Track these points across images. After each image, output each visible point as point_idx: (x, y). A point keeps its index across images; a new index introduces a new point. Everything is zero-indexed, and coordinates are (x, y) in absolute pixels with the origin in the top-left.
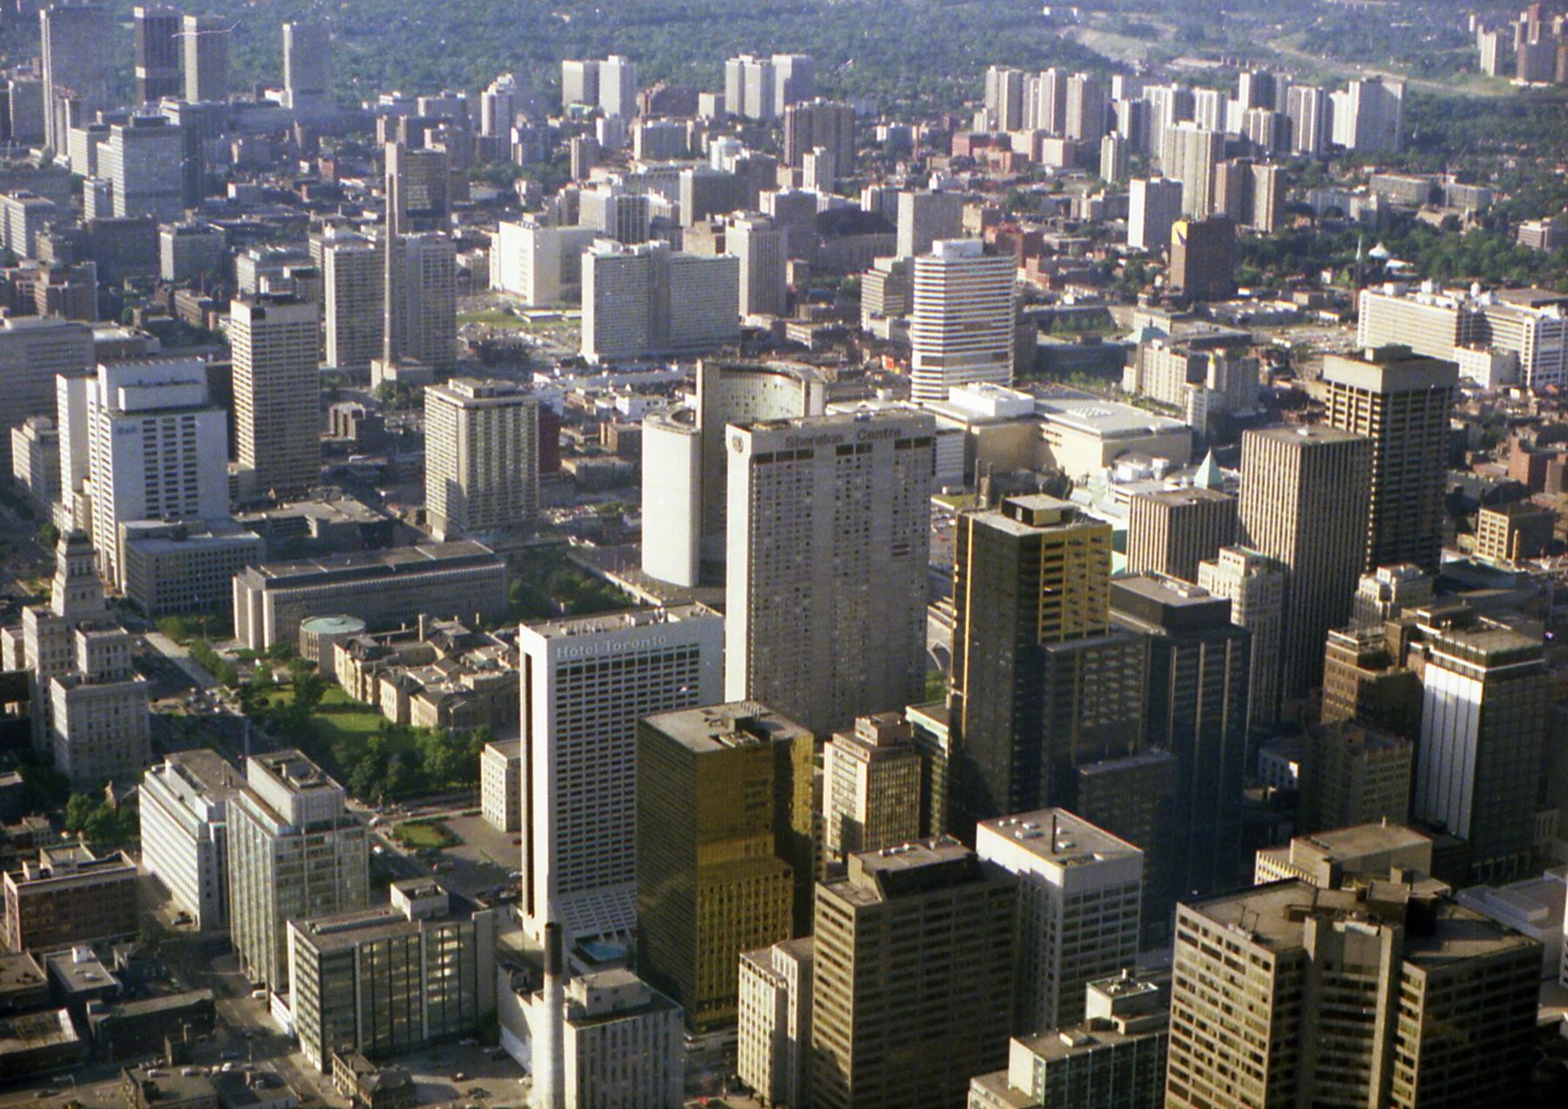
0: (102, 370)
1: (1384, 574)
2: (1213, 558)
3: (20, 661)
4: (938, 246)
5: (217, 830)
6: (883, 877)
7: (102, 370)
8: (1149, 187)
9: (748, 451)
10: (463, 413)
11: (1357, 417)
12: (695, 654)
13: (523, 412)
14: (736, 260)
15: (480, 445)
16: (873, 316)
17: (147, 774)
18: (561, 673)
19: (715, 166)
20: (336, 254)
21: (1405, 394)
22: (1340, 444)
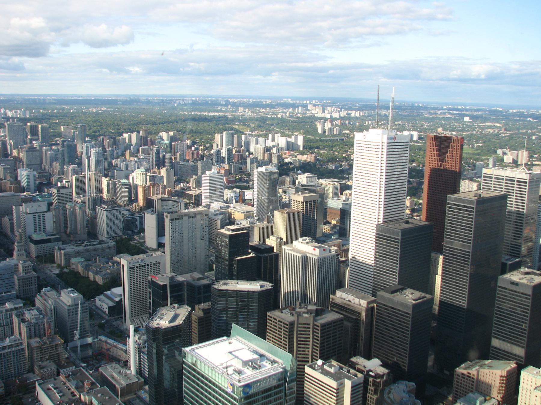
0: (23, 204)
2: (269, 238)
4: (207, 172)
6: (203, 310)
7: (23, 204)
8: (251, 159)
12: (159, 263)
14: (163, 176)
18: (130, 268)
22: (442, 278)
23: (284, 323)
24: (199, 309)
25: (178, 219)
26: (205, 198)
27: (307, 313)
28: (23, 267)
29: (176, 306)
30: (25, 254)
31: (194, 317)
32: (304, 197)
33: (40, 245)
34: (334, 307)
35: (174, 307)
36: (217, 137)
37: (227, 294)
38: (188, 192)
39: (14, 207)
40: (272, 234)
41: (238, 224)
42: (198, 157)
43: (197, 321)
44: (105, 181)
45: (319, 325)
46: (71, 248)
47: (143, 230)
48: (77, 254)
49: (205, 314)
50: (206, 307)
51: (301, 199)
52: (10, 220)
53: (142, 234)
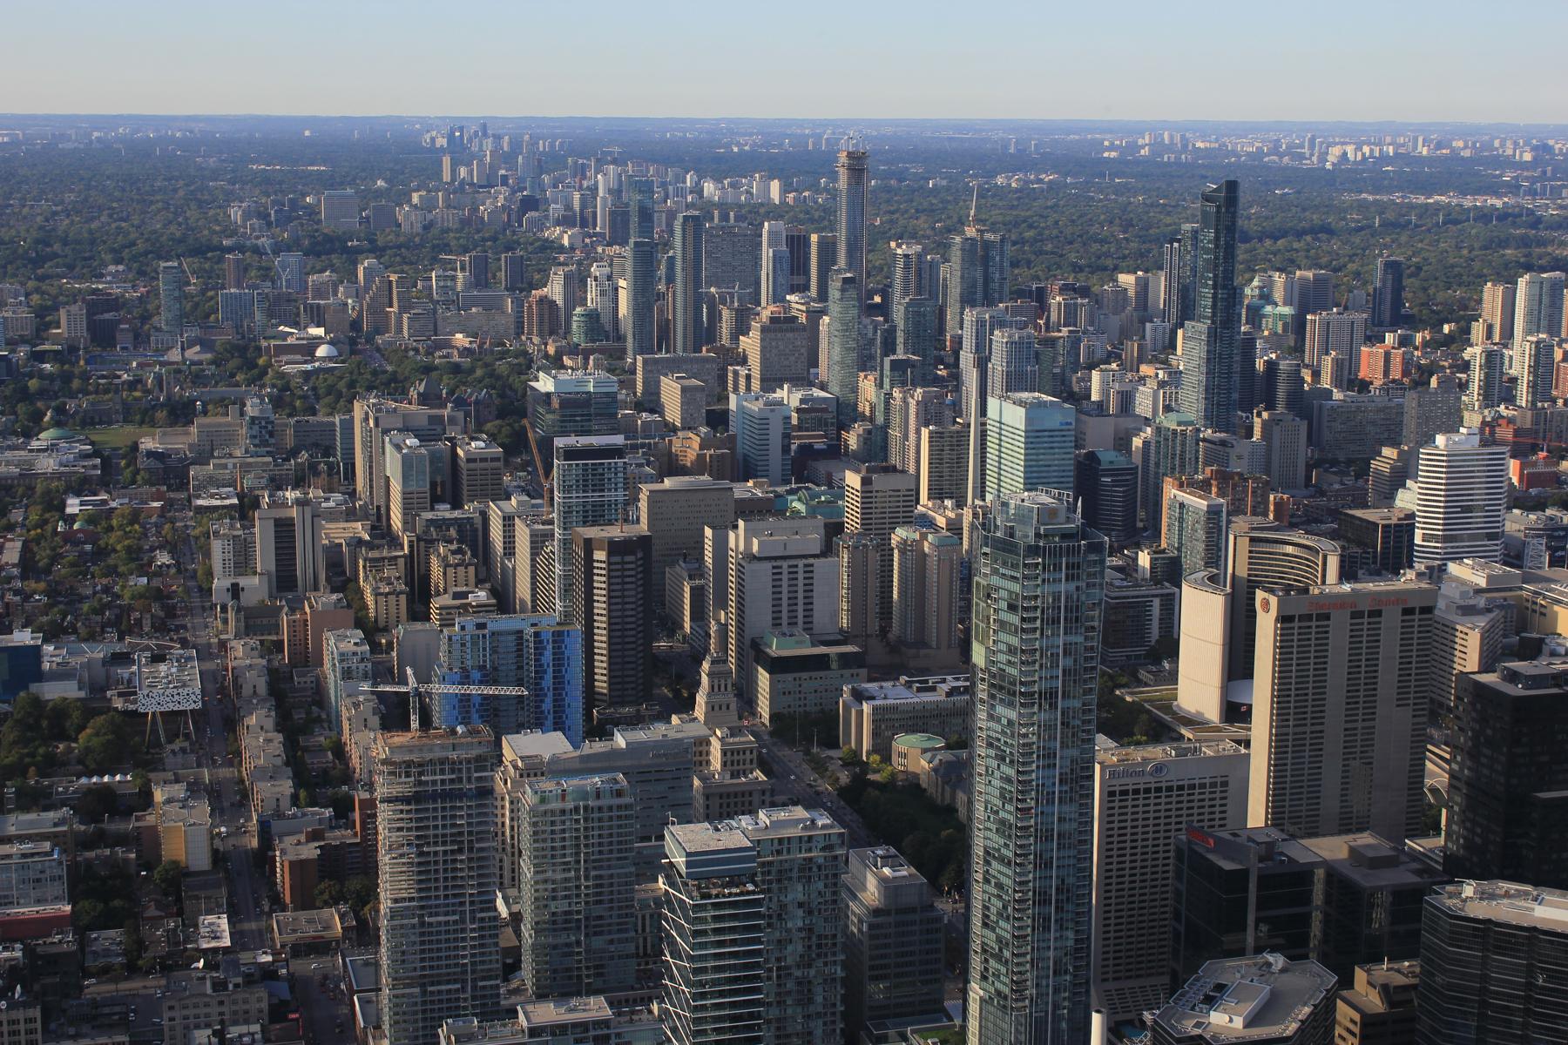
4: (1440, 440)
7: (741, 523)
12: (1225, 784)
18: (1112, 794)
20: (931, 432)
26: (1425, 538)
28: (724, 753)
29: (1277, 961)
30: (733, 706)
31: (1344, 1012)
33: (789, 677)
35: (1269, 965)
36: (1492, 295)
37: (1490, 934)
38: (1358, 513)
39: (708, 532)
41: (1553, 654)
42: (1405, 373)
43: (1356, 1030)
46: (897, 693)
47: (1169, 646)
48: (916, 721)
50: (1401, 980)
53: (1167, 665)
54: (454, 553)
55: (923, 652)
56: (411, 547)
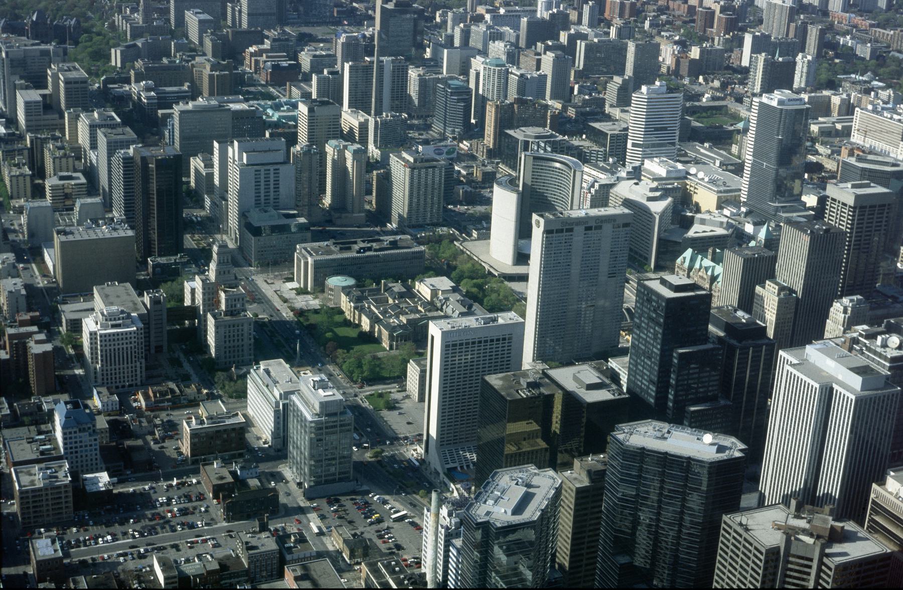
0: (236, 143)
1: (846, 301)
3: (193, 300)
4: (644, 89)
5: (284, 405)
7: (236, 143)
8: (755, 38)
9: (542, 228)
10: (408, 170)
11: (841, 216)
13: (437, 171)
14: (546, 76)
15: (416, 181)
16: (611, 106)
17: (252, 371)
18: (447, 346)
19: (539, 15)
20: (350, 67)
21: (865, 207)
23: (756, 549)
24: (581, 467)
25: (561, 231)
26: (634, 145)
27: (811, 535)
32: (858, 197)
34: (877, 513)
39: (216, 144)
40: (771, 275)
44: (413, 74)
45: (833, 567)
49: (592, 480)
51: (851, 201)
52: (206, 167)
54: (59, 148)
55: (344, 215)
56: (32, 142)
